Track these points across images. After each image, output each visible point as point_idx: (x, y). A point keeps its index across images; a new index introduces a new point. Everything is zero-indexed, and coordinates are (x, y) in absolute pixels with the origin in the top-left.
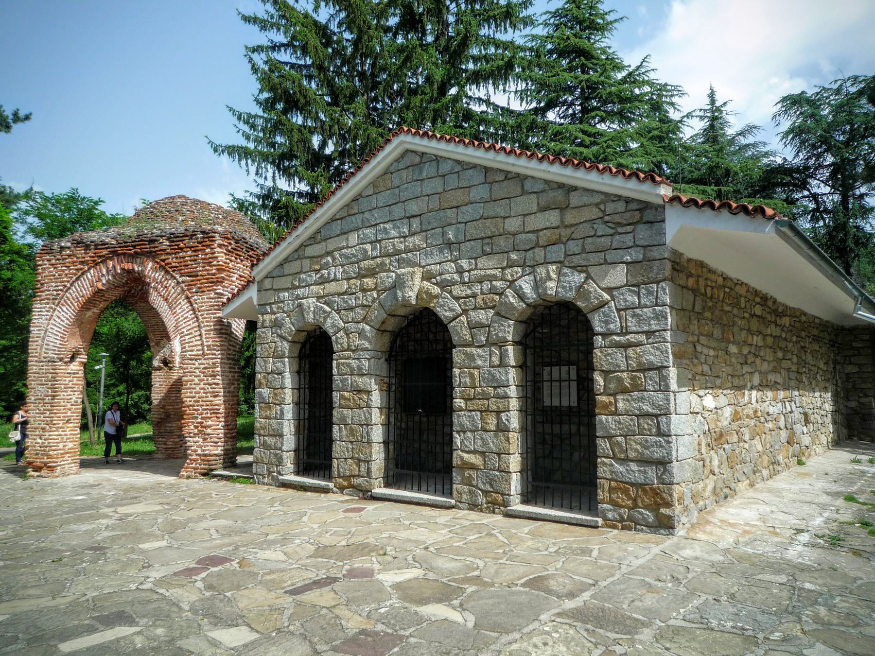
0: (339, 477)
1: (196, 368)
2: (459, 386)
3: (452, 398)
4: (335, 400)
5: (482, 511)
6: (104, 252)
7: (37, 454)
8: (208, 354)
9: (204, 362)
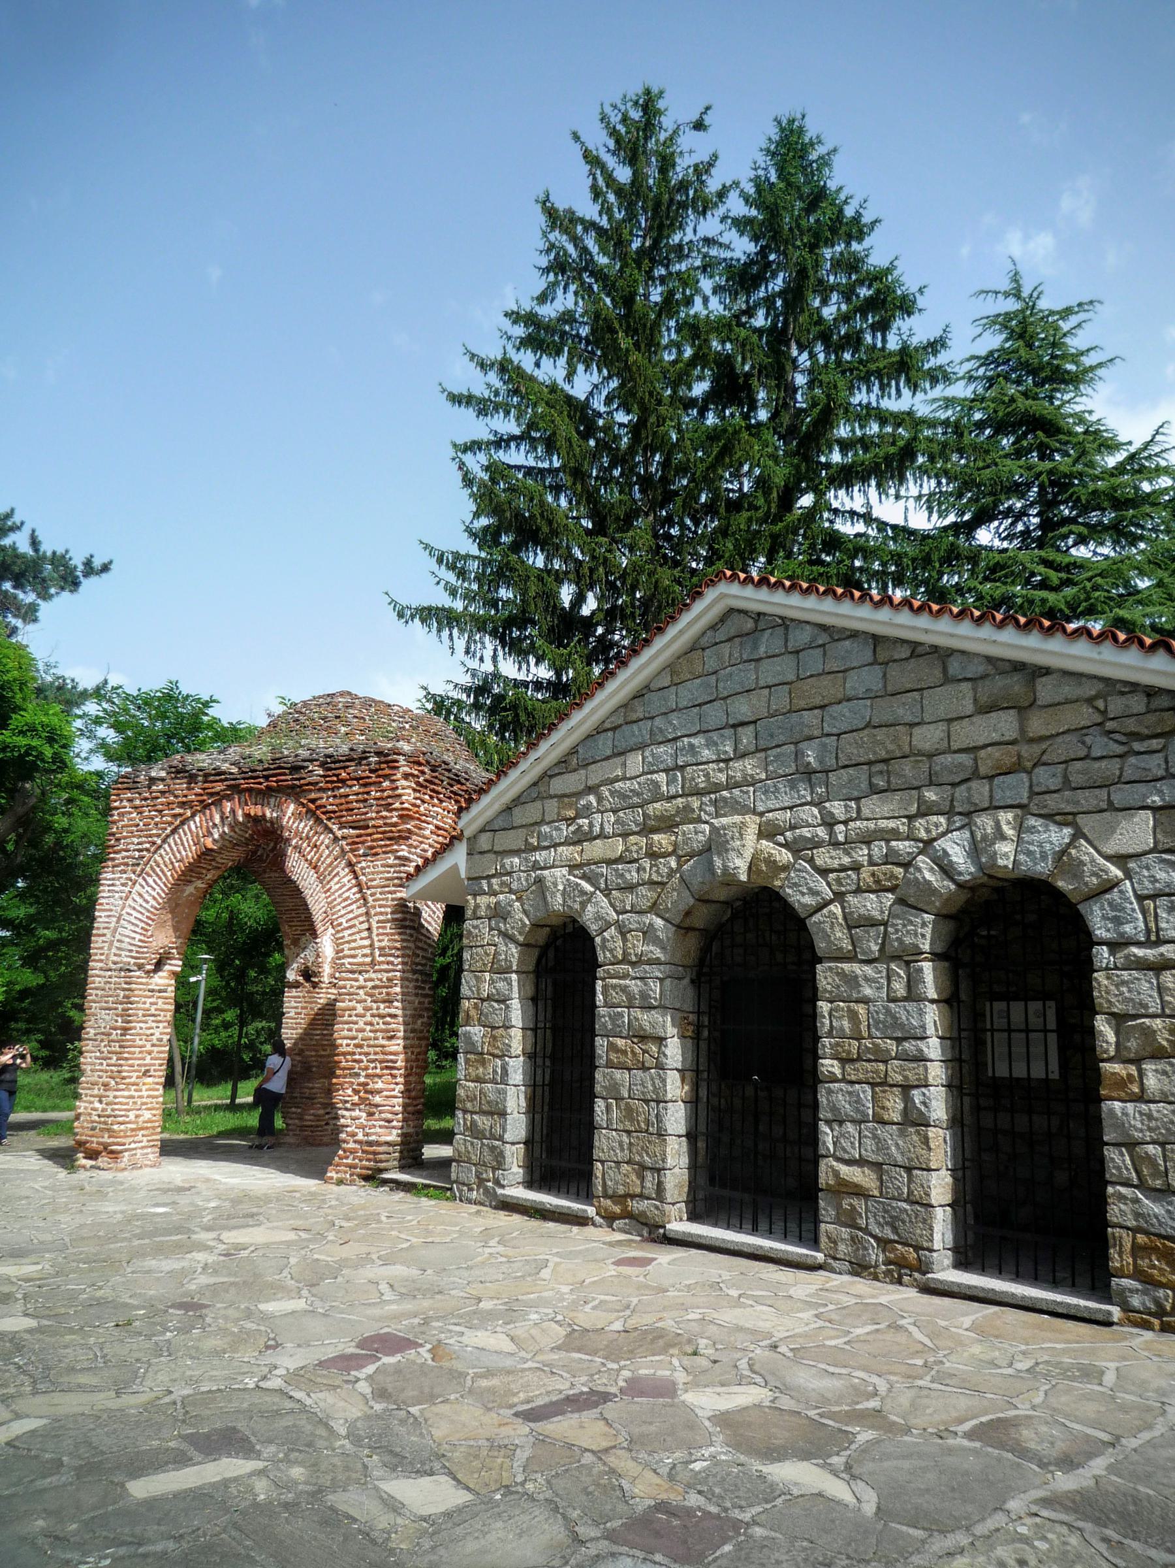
0: (606, 1196)
1: (359, 988)
2: (830, 1034)
3: (816, 1057)
4: (599, 1051)
5: (876, 1278)
6: (219, 787)
7: (93, 1129)
8: (380, 963)
9: (373, 976)
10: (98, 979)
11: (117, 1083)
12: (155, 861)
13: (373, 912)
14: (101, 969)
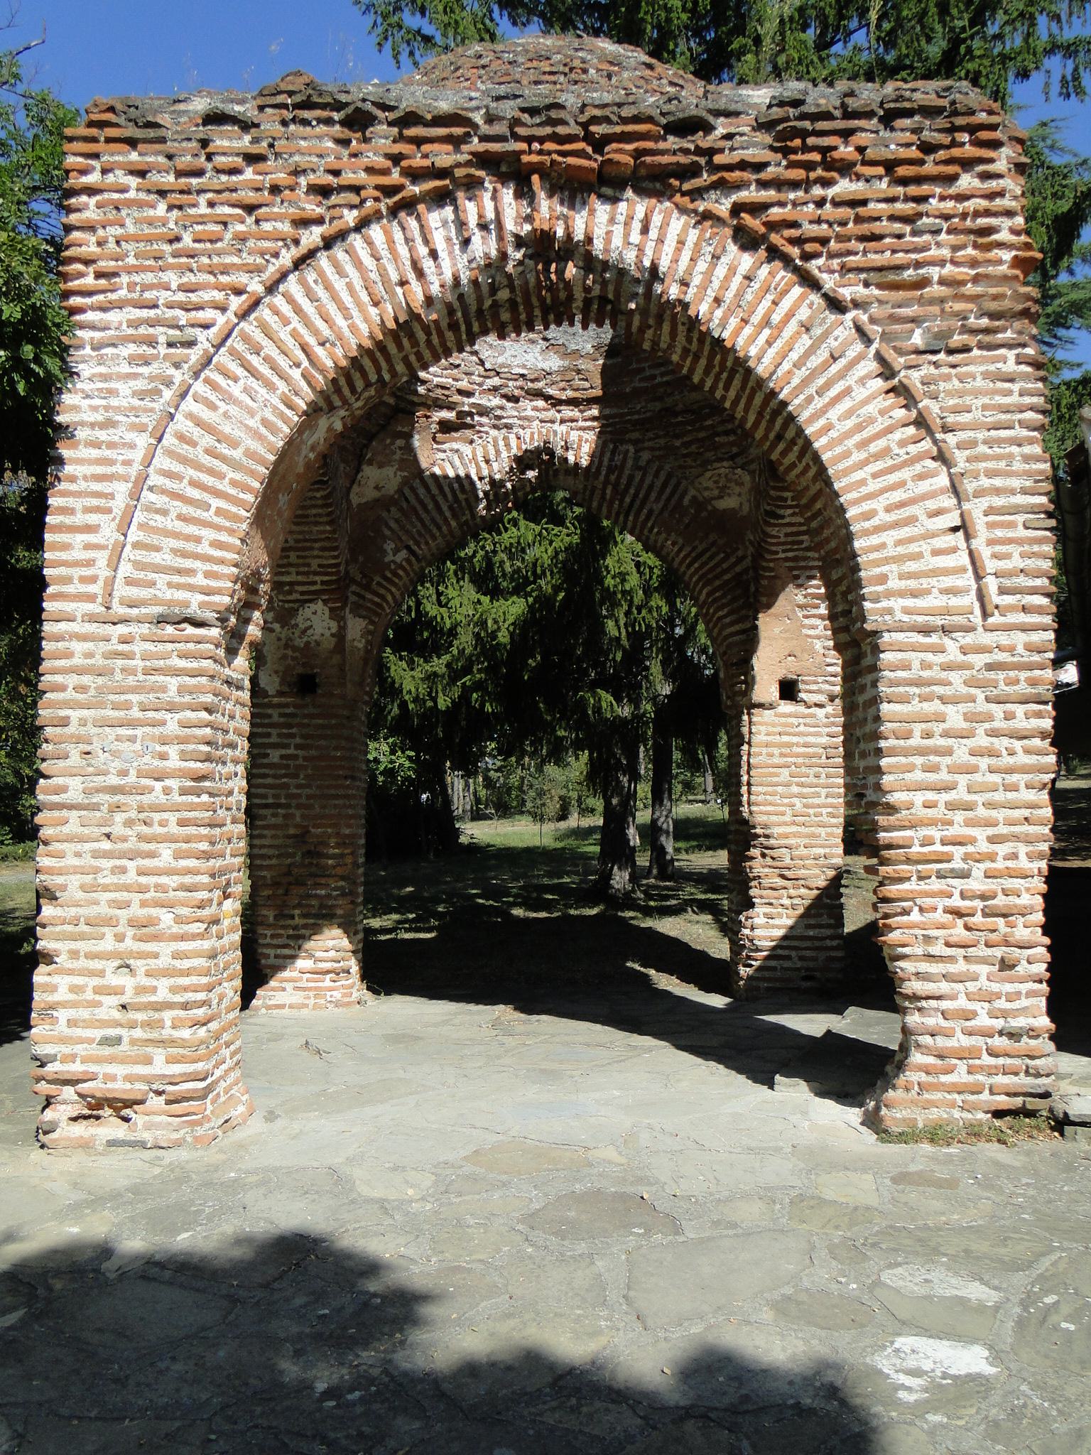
1: (947, 667)
10: (78, 647)
11: (179, 920)
12: (246, 338)
13: (969, 486)
14: (92, 618)
